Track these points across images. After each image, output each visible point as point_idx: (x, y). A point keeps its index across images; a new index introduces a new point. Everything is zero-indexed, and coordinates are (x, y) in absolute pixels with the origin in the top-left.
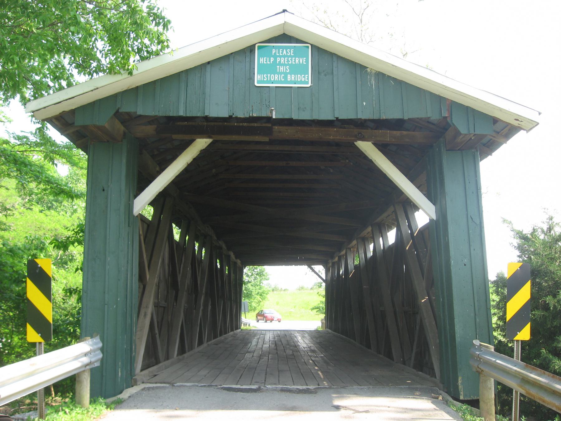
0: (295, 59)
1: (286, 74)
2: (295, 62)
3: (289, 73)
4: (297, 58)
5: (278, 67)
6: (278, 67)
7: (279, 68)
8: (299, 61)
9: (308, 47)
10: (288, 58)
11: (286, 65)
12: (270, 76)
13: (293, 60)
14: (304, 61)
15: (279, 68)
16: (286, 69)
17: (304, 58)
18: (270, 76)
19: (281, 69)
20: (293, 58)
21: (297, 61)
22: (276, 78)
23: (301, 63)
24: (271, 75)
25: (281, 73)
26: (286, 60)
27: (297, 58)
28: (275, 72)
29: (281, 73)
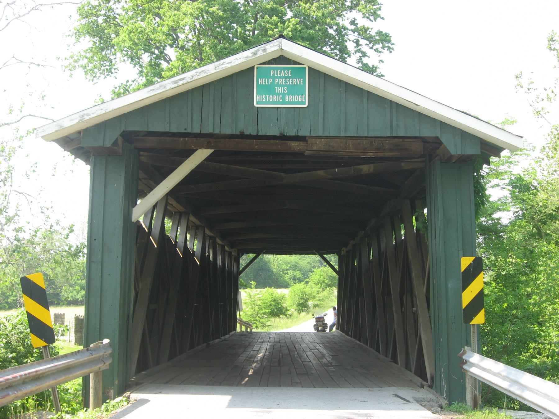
0: (293, 81)
1: (284, 95)
2: (292, 82)
3: (287, 94)
4: (294, 79)
5: (276, 88)
6: (276, 88)
7: (278, 89)
8: (297, 82)
9: (305, 68)
10: (286, 79)
11: (284, 86)
12: (269, 97)
13: (291, 81)
14: (301, 81)
15: (278, 89)
16: (284, 91)
17: (301, 79)
18: (269, 97)
19: (279, 89)
20: (291, 79)
21: (294, 82)
22: (275, 98)
23: (298, 84)
24: (269, 96)
25: (278, 94)
26: (284, 81)
27: (294, 79)
28: (273, 92)
29: (279, 94)
